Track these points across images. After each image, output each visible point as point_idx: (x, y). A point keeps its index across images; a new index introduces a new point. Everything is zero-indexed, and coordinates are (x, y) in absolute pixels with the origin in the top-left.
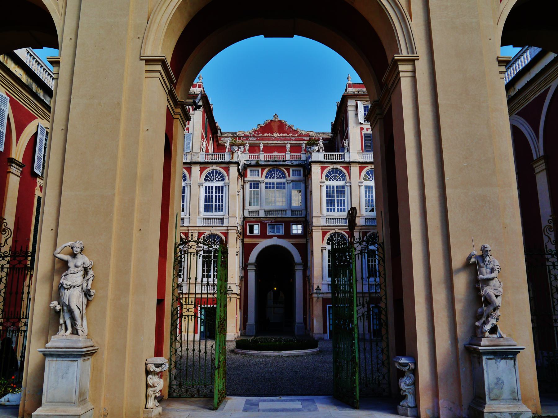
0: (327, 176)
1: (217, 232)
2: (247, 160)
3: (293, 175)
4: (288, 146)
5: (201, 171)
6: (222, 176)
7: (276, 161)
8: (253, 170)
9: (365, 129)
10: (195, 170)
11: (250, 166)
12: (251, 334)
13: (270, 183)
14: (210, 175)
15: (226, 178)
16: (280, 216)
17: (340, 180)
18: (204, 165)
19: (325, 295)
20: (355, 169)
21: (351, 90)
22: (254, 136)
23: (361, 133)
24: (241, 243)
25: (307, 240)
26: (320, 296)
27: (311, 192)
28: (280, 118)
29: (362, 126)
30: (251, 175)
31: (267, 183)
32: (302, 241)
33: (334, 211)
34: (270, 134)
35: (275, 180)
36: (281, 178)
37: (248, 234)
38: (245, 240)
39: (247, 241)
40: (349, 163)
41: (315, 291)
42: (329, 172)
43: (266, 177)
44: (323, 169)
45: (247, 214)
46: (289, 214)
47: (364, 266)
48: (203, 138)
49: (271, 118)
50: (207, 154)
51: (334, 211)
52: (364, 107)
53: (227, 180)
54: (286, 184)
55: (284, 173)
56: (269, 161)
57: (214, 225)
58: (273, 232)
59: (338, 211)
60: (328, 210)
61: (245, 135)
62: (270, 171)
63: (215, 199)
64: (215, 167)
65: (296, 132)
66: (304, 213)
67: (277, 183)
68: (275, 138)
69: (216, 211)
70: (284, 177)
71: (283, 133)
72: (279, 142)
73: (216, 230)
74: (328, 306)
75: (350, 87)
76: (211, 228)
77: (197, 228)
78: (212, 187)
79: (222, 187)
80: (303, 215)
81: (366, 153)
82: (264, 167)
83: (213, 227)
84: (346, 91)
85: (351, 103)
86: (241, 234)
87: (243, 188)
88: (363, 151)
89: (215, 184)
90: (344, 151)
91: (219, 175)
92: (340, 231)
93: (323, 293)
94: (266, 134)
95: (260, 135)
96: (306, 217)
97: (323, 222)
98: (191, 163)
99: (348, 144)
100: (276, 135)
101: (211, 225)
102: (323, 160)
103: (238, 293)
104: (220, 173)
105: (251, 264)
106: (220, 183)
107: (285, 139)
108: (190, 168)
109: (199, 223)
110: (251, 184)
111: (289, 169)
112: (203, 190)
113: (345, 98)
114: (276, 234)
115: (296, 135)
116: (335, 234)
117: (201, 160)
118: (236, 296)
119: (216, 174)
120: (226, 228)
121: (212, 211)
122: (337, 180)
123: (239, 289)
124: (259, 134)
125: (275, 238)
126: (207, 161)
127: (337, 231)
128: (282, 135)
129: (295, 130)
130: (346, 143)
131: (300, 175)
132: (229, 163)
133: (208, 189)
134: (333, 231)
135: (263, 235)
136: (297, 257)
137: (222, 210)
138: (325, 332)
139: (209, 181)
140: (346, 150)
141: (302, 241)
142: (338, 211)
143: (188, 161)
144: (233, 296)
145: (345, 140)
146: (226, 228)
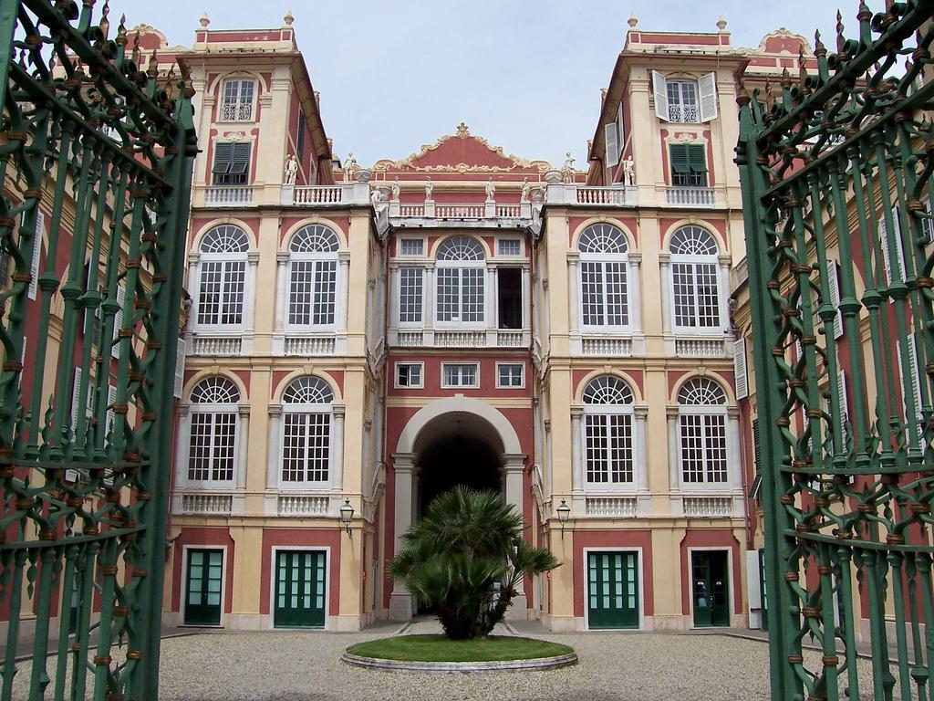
0: (582, 239)
1: (318, 372)
3: (501, 252)
5: (284, 226)
6: (334, 239)
7: (462, 220)
8: (410, 241)
10: (270, 225)
11: (403, 229)
12: (403, 618)
13: (448, 271)
16: (472, 346)
17: (615, 251)
18: (285, 213)
19: (579, 525)
20: (649, 226)
21: (637, 48)
23: (663, 143)
24: (380, 408)
25: (534, 400)
26: (567, 525)
27: (545, 282)
28: (473, 132)
29: (663, 127)
30: (404, 253)
31: (440, 272)
32: (525, 403)
33: (601, 323)
34: (449, 168)
35: (460, 264)
36: (473, 259)
37: (397, 385)
38: (387, 401)
39: (393, 402)
40: (637, 209)
41: (555, 515)
42: (588, 231)
43: (440, 257)
44: (572, 223)
45: (393, 342)
46: (492, 342)
47: (673, 455)
48: (290, 151)
49: (454, 133)
50: (298, 188)
51: (601, 323)
52: (669, 86)
53: (343, 248)
54: (485, 271)
55: (480, 248)
56: (445, 220)
57: (310, 354)
58: (455, 382)
59: (610, 322)
60: (586, 322)
62: (446, 242)
63: (311, 296)
64: (315, 218)
65: (508, 162)
66: (527, 338)
67: (465, 272)
68: (462, 174)
69: (316, 321)
70: (481, 257)
73: (315, 366)
74: (586, 550)
75: (635, 39)
76: (306, 361)
77: (270, 361)
78: (309, 264)
79: (334, 265)
80: (526, 344)
81: (676, 188)
82: (433, 233)
83: (309, 358)
84: (626, 47)
85: (637, 76)
86: (378, 381)
87: (387, 280)
88: (667, 184)
89: (314, 257)
90: (622, 180)
91: (325, 236)
92: (616, 371)
93: (575, 520)
94: (440, 167)
95: (427, 168)
96: (532, 349)
97: (576, 350)
98: (260, 209)
99: (633, 168)
100: (463, 168)
101: (305, 354)
102: (574, 202)
103: (370, 519)
104: (328, 233)
105: (404, 456)
106: (330, 256)
108: (259, 219)
109: (278, 349)
110: (404, 274)
111: (493, 238)
112: (286, 272)
113: (625, 64)
114: (460, 385)
115: (508, 169)
116: (602, 377)
117: (288, 202)
118: (360, 524)
119: (319, 234)
120: (341, 361)
121: (307, 322)
122: (609, 251)
123: (371, 510)
125: (459, 396)
126: (298, 203)
127: (608, 370)
128: (475, 168)
129: (507, 160)
130: (628, 164)
131: (518, 253)
132: (348, 208)
133: (300, 271)
134: (599, 371)
135: (433, 390)
136: (512, 444)
137: (331, 321)
138: (578, 612)
139: (302, 250)
140: (627, 182)
141: (525, 403)
142: (610, 322)
143: (254, 204)
144: (352, 525)
145: (626, 158)
146: (341, 361)
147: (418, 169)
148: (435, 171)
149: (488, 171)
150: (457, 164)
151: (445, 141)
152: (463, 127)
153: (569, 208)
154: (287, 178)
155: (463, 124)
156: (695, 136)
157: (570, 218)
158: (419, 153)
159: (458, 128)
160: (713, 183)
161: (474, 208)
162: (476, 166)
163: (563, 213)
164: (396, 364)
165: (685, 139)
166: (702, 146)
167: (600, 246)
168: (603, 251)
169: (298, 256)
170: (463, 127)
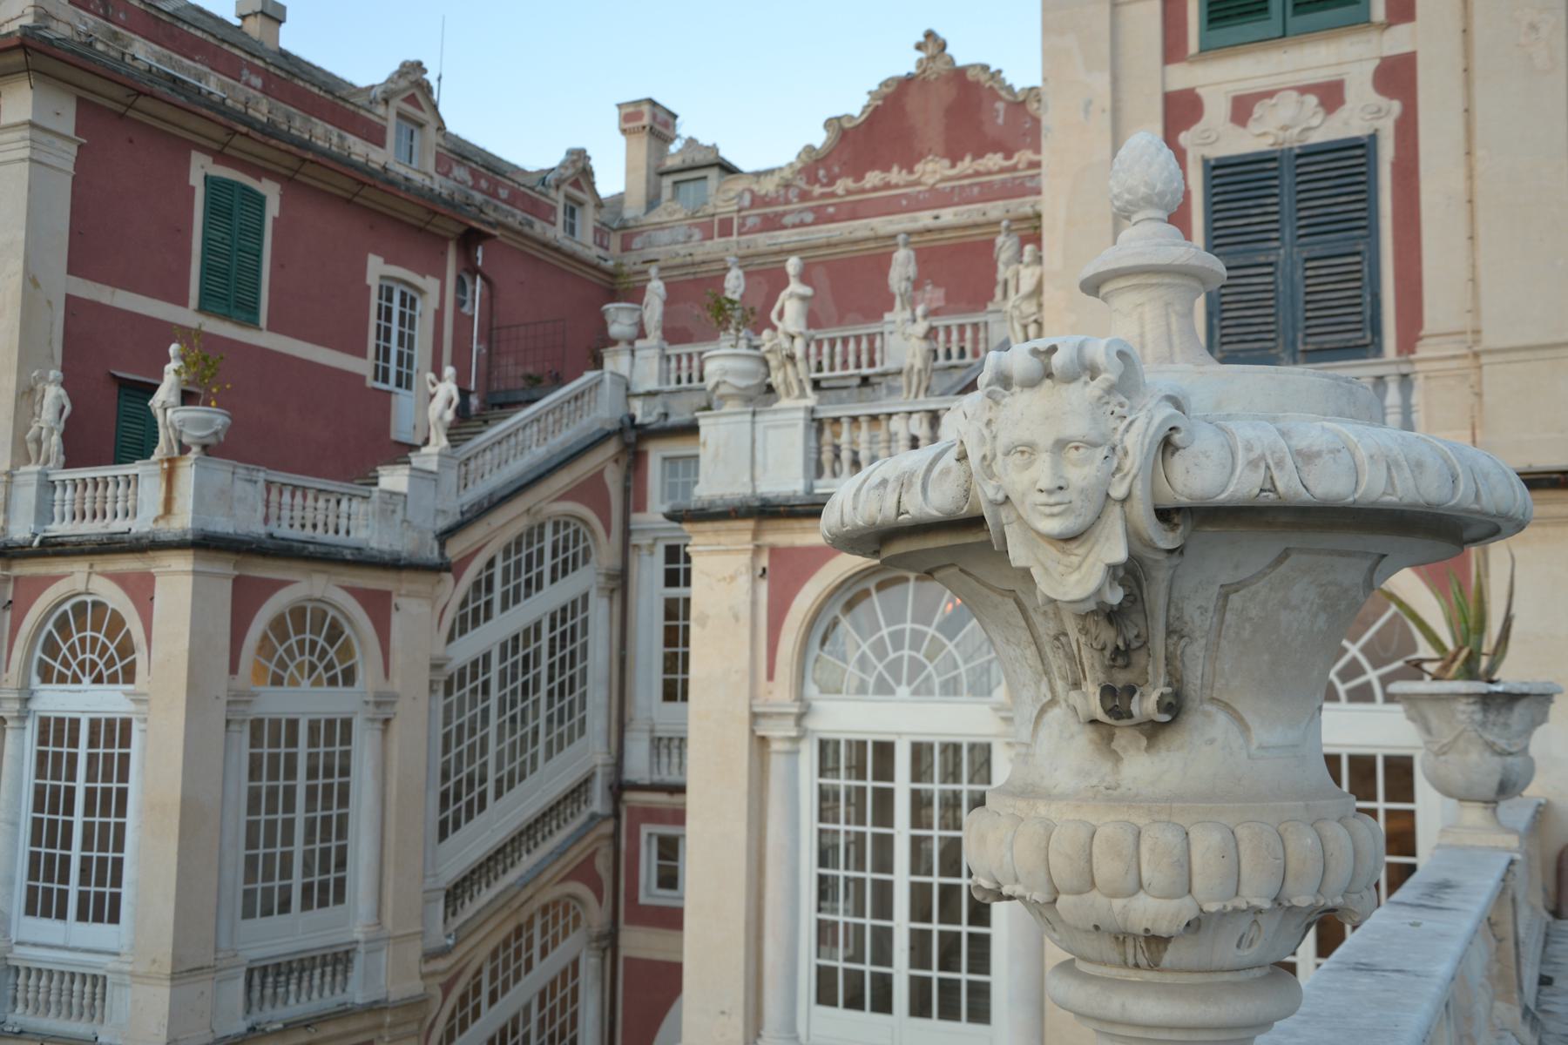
2: (651, 394)
4: (902, 267)
9: (1216, 109)
14: (66, 636)
15: (140, 657)
22: (804, 196)
28: (963, 54)
34: (896, 175)
49: (906, 63)
61: (758, 201)
64: (78, 580)
71: (978, 155)
72: (948, 216)
94: (873, 178)
95: (841, 186)
100: (933, 170)
104: (118, 621)
107: (989, 193)
112: (23, 745)
124: (831, 182)
128: (966, 165)
139: (62, 679)
147: (817, 190)
148: (863, 191)
149: (1002, 170)
150: (918, 160)
151: (886, 98)
152: (932, 43)
153: (767, 512)
154: (32, 447)
155: (930, 35)
156: (1331, 95)
157: (774, 551)
158: (819, 138)
159: (919, 47)
160: (1409, 339)
161: (858, 339)
162: (968, 159)
163: (740, 535)
164: (645, 830)
165: (1288, 124)
166: (1361, 150)
167: (894, 667)
168: (903, 691)
169: (55, 700)
170: (932, 43)
